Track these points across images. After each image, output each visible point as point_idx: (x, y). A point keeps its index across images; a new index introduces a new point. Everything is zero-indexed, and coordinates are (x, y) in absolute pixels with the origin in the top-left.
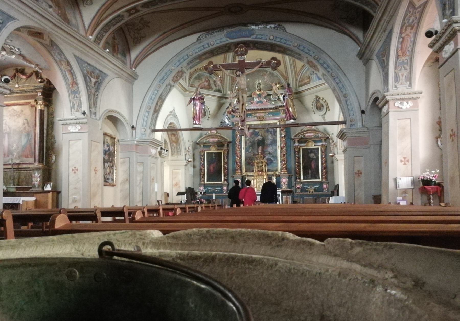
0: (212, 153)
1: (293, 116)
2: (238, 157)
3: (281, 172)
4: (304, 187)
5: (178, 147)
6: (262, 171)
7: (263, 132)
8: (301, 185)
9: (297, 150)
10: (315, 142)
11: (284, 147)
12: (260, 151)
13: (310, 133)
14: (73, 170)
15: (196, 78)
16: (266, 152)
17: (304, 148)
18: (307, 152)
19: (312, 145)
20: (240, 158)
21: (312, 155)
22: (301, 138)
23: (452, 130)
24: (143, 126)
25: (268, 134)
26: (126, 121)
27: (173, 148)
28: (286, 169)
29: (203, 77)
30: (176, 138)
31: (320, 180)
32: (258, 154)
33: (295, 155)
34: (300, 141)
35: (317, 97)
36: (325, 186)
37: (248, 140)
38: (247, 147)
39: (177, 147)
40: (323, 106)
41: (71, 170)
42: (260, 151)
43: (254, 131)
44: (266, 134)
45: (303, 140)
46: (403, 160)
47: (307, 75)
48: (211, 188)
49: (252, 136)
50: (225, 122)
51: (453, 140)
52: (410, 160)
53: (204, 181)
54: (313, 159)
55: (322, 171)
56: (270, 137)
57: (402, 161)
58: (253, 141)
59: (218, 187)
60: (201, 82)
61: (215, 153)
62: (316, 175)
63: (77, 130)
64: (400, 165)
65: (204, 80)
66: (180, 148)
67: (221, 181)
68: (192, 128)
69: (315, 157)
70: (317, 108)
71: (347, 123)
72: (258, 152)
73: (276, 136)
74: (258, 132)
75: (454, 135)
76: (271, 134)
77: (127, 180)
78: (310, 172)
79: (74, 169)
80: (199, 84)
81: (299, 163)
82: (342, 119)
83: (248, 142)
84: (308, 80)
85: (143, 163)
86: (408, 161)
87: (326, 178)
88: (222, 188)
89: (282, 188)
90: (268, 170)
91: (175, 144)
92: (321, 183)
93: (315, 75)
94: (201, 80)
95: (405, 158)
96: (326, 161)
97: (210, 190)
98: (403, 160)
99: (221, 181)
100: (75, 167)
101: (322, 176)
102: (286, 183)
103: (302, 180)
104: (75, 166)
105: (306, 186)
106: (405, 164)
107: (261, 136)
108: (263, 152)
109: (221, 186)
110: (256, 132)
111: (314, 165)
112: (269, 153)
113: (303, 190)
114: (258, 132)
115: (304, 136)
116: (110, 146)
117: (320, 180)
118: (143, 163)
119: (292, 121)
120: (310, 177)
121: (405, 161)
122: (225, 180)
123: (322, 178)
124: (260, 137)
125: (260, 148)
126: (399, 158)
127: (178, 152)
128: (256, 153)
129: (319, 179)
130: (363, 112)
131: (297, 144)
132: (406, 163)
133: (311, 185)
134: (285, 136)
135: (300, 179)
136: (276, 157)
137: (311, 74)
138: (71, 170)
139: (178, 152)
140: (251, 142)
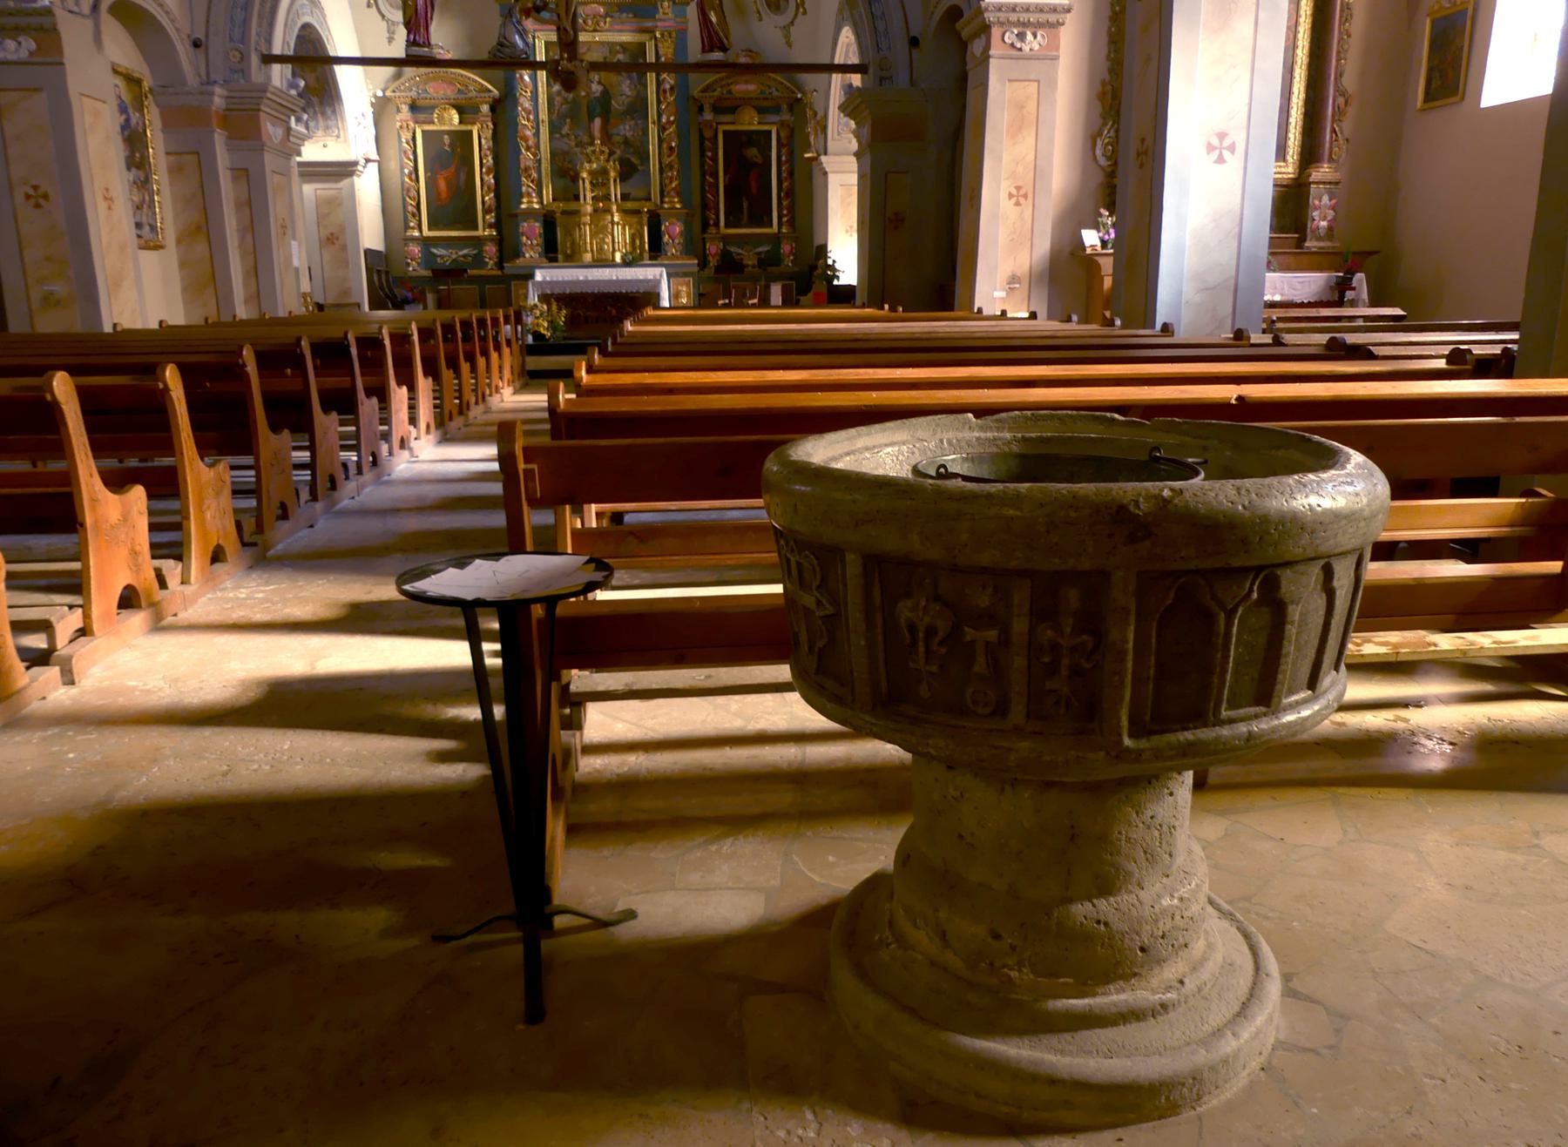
1: (720, 40)
2: (528, 149)
4: (730, 253)
6: (607, 197)
9: (708, 134)
10: (761, 111)
11: (669, 122)
12: (597, 133)
14: (28, 197)
18: (737, 141)
19: (749, 121)
20: (535, 155)
21: (752, 153)
22: (720, 99)
23: (1143, 140)
24: (231, 40)
26: (172, 21)
32: (592, 144)
33: (702, 154)
34: (717, 109)
36: (786, 248)
37: (559, 93)
38: (554, 117)
41: (19, 197)
42: (597, 133)
45: (727, 107)
46: (1014, 192)
50: (514, 45)
51: (1141, 166)
52: (1030, 196)
55: (780, 203)
57: (1011, 196)
58: (574, 100)
62: (760, 215)
63: (23, 54)
64: (1007, 206)
67: (476, 228)
68: (403, 55)
69: (759, 160)
71: (871, 70)
75: (1146, 153)
77: (198, 228)
78: (745, 205)
79: (31, 192)
81: (715, 175)
82: (854, 59)
83: (558, 99)
85: (246, 170)
86: (1025, 196)
87: (791, 223)
88: (481, 252)
92: (776, 239)
95: (1018, 188)
96: (791, 174)
97: (442, 257)
98: (1014, 192)
100: (35, 188)
101: (780, 217)
103: (724, 230)
104: (34, 182)
106: (1018, 204)
112: (626, 142)
115: (730, 92)
116: (130, 110)
118: (246, 170)
119: (717, 56)
121: (1018, 196)
123: (780, 224)
125: (598, 122)
126: (1006, 187)
128: (586, 139)
130: (914, 42)
131: (708, 116)
132: (1022, 200)
134: (672, 88)
135: (717, 224)
136: (645, 157)
138: (19, 197)
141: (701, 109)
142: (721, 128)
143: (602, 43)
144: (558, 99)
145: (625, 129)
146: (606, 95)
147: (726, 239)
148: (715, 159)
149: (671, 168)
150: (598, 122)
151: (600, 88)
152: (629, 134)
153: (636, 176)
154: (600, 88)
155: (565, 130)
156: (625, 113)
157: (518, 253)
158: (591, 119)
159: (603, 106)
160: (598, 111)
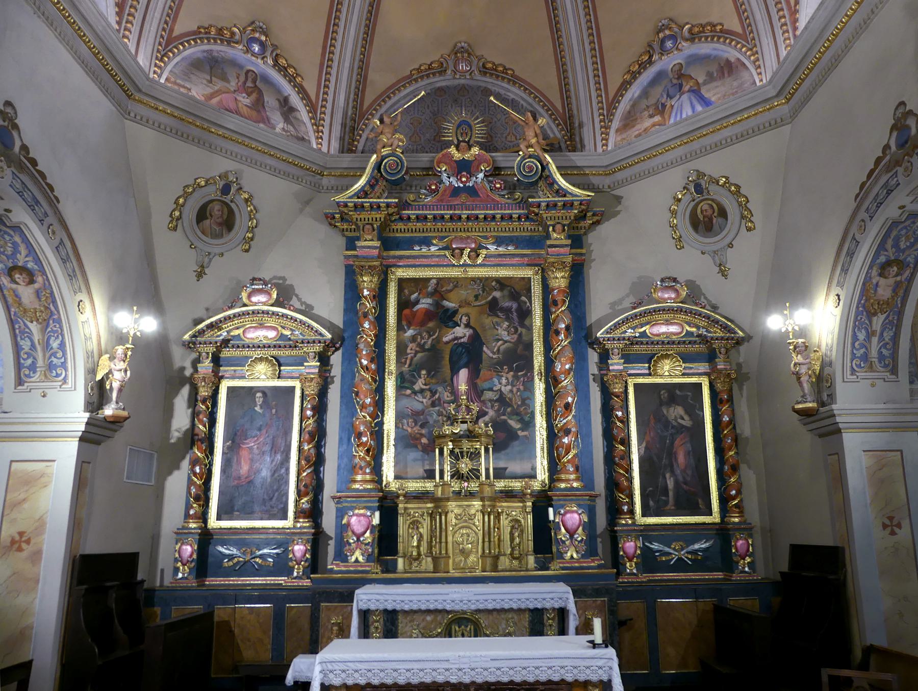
0: (251, 391)
2: (363, 407)
3: (552, 479)
5: (55, 344)
7: (473, 312)
8: (640, 544)
9: (618, 389)
10: (686, 358)
13: (668, 323)
15: (196, 65)
16: (488, 395)
17: (641, 380)
19: (669, 372)
20: (374, 416)
22: (632, 342)
25: (496, 319)
27: (25, 345)
28: (577, 469)
29: (231, 73)
30: (37, 293)
31: (715, 518)
34: (628, 359)
35: (700, 174)
37: (413, 339)
38: (405, 368)
39: (47, 346)
40: (723, 213)
42: (463, 387)
43: (437, 305)
44: (488, 321)
47: (652, 101)
48: (234, 551)
49: (431, 325)
53: (204, 517)
54: (681, 429)
56: (502, 335)
59: (267, 544)
60: (219, 85)
61: (264, 391)
65: (233, 84)
66: (62, 346)
69: (687, 422)
70: (696, 224)
72: (455, 393)
73: (530, 329)
74: (455, 312)
76: (508, 319)
80: (209, 91)
81: (626, 442)
83: (411, 347)
84: (657, 119)
88: (286, 551)
89: (561, 556)
90: (500, 474)
91: (34, 327)
93: (685, 97)
94: (225, 79)
97: (231, 557)
99: (285, 517)
101: (724, 500)
102: (580, 535)
103: (641, 520)
105: (655, 546)
107: (468, 325)
108: (476, 391)
109: (284, 540)
110: (447, 310)
111: (687, 454)
112: (502, 400)
113: (648, 561)
114: (455, 312)
117: (715, 518)
120: (671, 506)
122: (298, 514)
124: (461, 332)
125: (463, 374)
127: (51, 367)
129: (710, 513)
133: (677, 539)
135: (632, 512)
137: (670, 97)
139: (51, 367)
140: (422, 347)
141: (604, 357)
142: (631, 382)
143: (474, 279)
144: (411, 347)
145: (503, 383)
146: (476, 343)
147: (647, 532)
148: (625, 421)
149: (567, 432)
150: (463, 374)
151: (468, 332)
152: (506, 389)
153: (516, 446)
154: (468, 332)
155: (419, 384)
156: (500, 363)
157: (341, 556)
158: (455, 371)
159: (470, 354)
160: (464, 360)
